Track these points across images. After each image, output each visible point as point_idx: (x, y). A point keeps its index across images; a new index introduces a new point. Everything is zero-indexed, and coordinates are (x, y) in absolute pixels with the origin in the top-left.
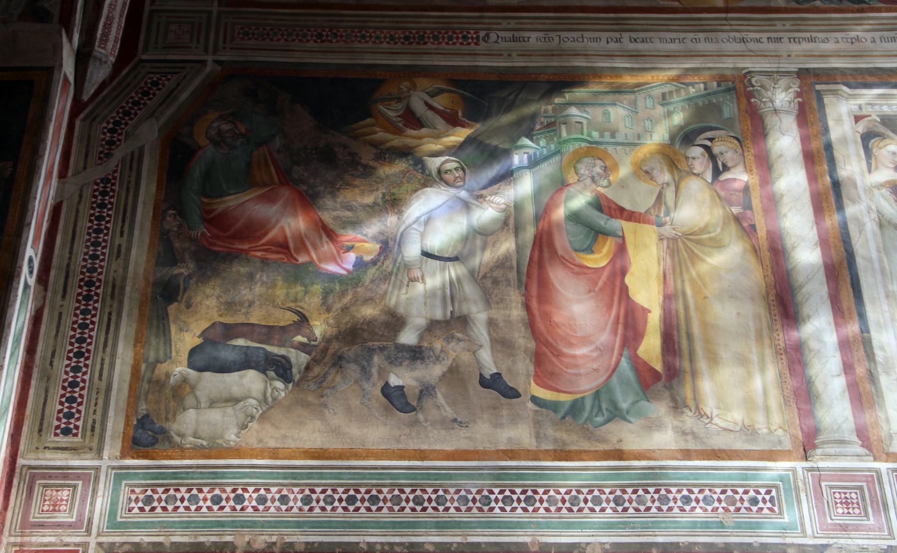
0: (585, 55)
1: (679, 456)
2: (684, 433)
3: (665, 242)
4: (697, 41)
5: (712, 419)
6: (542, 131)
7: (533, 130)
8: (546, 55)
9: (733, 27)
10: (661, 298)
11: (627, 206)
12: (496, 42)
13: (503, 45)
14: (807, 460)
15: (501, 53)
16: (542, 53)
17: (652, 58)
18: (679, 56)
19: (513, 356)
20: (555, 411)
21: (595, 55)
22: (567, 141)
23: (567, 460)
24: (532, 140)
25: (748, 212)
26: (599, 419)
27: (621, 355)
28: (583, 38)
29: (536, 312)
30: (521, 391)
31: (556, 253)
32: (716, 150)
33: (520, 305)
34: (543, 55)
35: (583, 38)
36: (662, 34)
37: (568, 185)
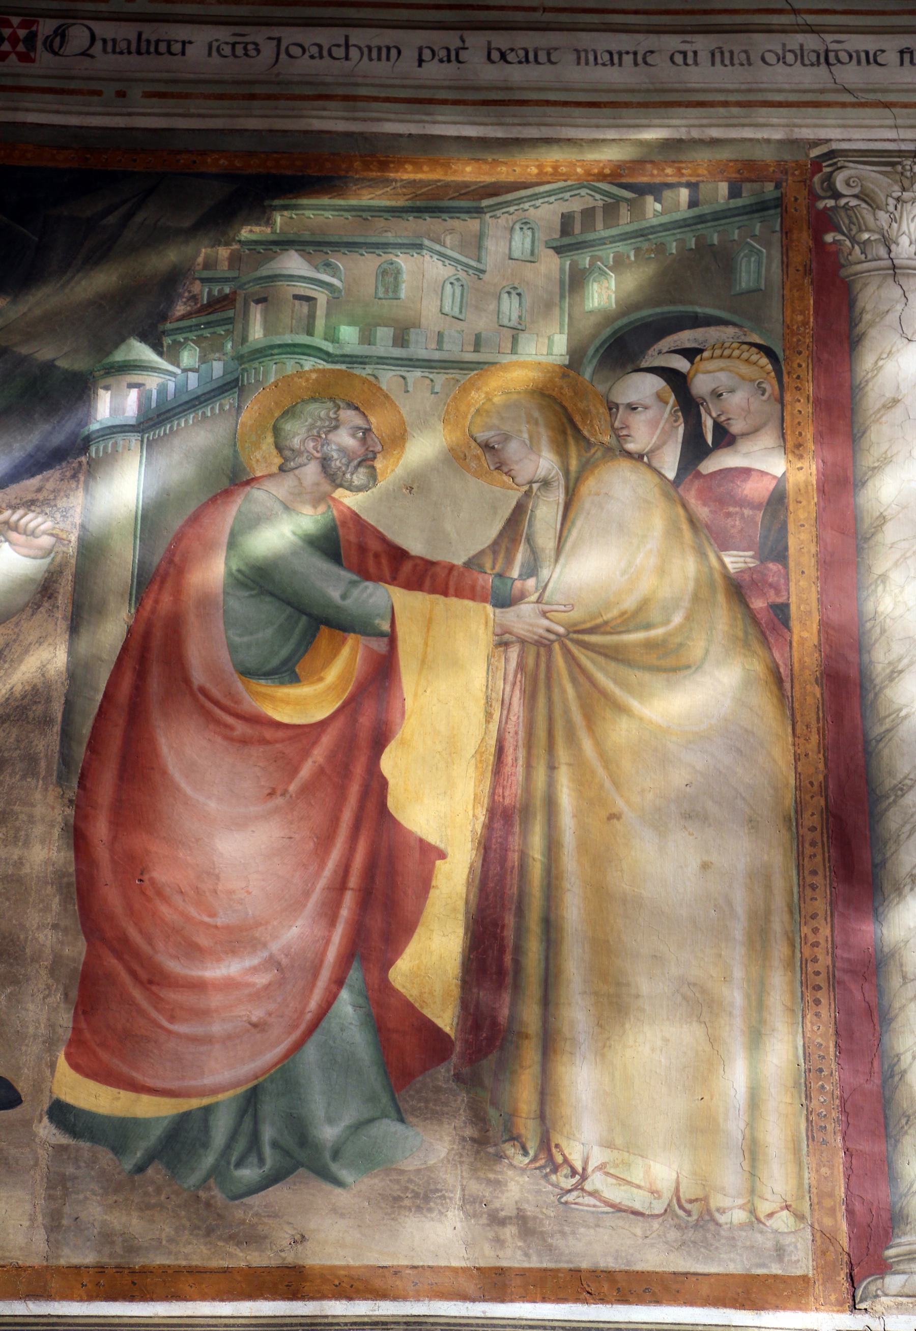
0: (346, 98)
1: (470, 1287)
2: (496, 1220)
3: (514, 653)
4: (687, 58)
5: (584, 1178)
6: (194, 321)
7: (164, 317)
8: (232, 97)
9: (800, 20)
10: (482, 817)
11: (415, 546)
12: (84, 54)
13: (105, 62)
14: (854, 1308)
15: (94, 86)
16: (217, 89)
17: (549, 110)
18: (627, 105)
19: (15, 981)
20: (119, 1149)
21: (376, 99)
22: (262, 353)
23: (131, 1298)
24: (157, 348)
25: (773, 567)
26: (248, 1174)
27: (339, 982)
28: (347, 46)
29: (102, 853)
30: (22, 1087)
31: (187, 681)
32: (701, 385)
33: (56, 832)
34: (221, 97)
35: (347, 46)
36: (585, 39)
37: (248, 483)
